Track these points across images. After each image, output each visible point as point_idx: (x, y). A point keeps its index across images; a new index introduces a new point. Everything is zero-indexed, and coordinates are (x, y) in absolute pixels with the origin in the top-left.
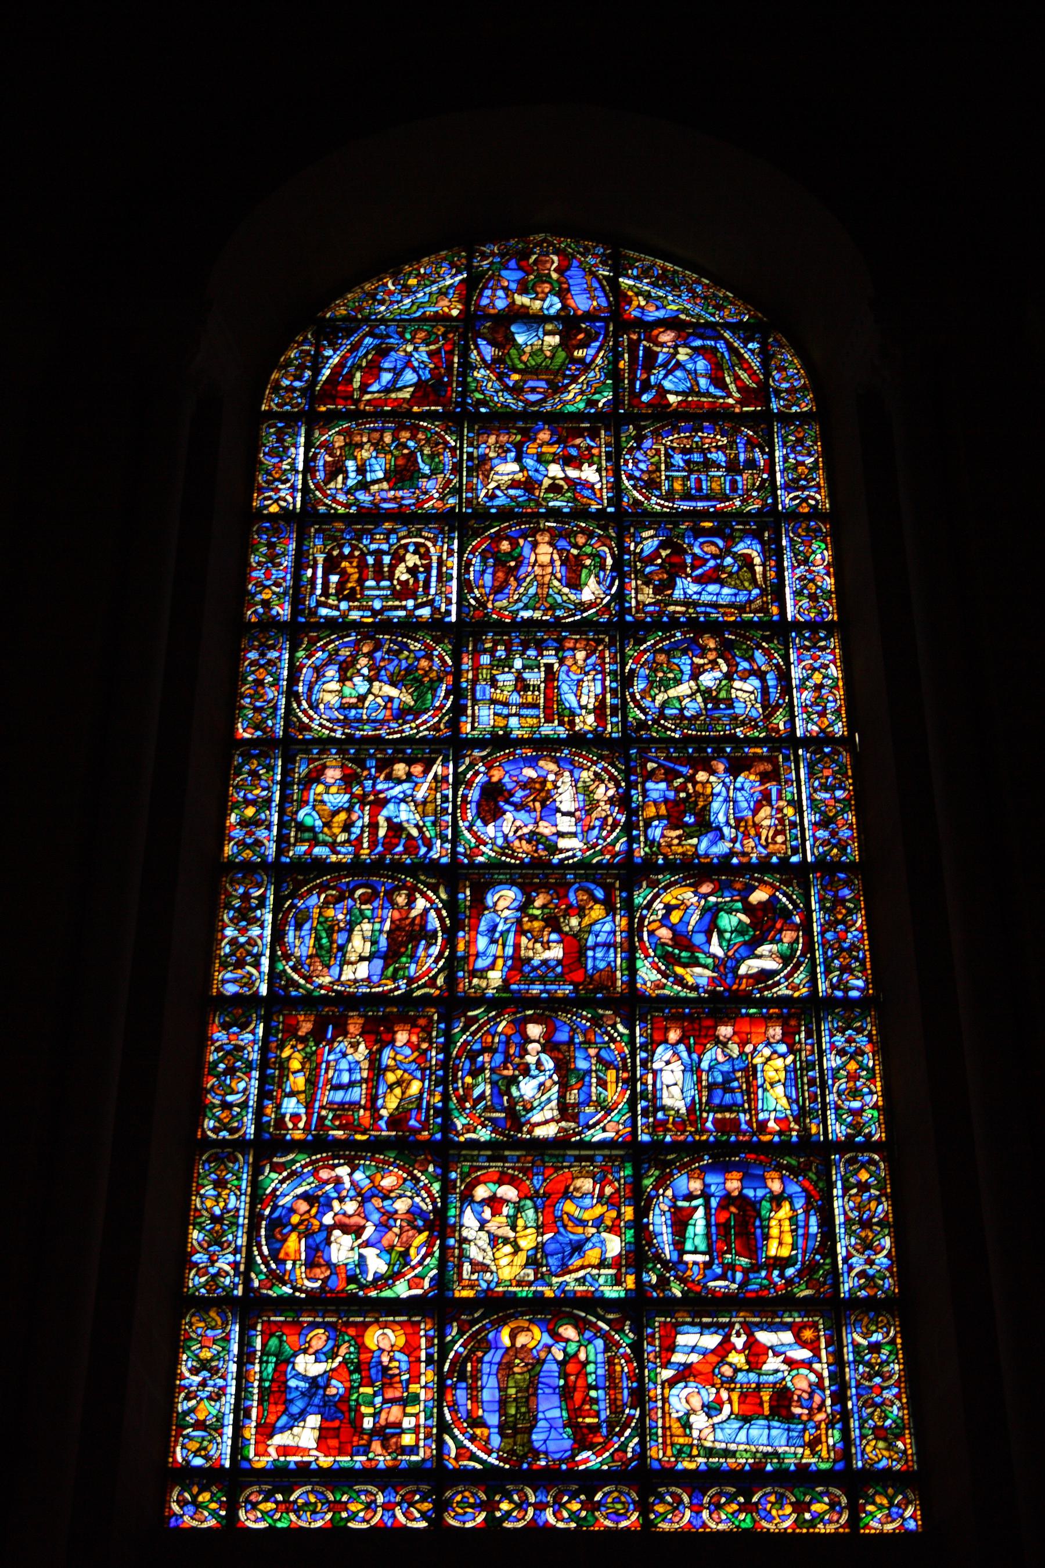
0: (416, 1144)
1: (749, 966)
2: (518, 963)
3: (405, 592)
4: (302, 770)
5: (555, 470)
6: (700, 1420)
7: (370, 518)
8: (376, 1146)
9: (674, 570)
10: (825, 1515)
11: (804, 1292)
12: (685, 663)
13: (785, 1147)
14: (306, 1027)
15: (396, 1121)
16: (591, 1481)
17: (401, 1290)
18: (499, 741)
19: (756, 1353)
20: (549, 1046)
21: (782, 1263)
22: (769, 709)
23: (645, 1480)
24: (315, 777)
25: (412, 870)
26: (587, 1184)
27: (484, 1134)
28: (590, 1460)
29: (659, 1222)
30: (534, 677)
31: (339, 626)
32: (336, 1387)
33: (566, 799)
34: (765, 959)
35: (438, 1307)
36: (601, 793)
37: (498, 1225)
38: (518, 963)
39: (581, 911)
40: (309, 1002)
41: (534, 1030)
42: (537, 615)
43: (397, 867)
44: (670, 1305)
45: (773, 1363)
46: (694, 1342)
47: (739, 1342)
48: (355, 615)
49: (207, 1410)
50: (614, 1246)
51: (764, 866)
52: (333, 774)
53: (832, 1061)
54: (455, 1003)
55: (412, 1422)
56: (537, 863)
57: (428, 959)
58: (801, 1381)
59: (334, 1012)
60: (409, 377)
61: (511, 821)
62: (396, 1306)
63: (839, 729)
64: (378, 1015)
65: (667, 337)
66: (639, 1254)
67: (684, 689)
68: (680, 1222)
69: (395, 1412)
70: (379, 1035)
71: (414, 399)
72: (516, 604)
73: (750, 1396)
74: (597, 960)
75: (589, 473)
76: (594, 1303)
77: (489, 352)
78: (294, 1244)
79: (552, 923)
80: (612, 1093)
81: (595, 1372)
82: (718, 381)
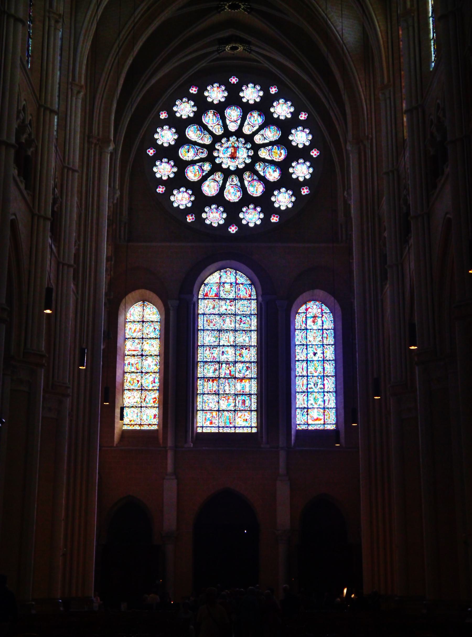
0: (217, 394)
1: (246, 374)
2: (225, 373)
3: (214, 325)
4: (205, 349)
5: (230, 307)
6: (239, 422)
7: (211, 314)
8: (213, 394)
9: (241, 322)
10: (249, 430)
11: (249, 409)
12: (241, 335)
13: (248, 394)
14: (206, 381)
15: (215, 391)
16: (231, 427)
17: (215, 409)
18: (224, 346)
19: (245, 415)
20: (228, 383)
21: (247, 406)
22: (249, 341)
23: (235, 427)
24: (206, 350)
25: (215, 362)
26: (231, 398)
27: (222, 393)
28: (231, 426)
29: (237, 402)
30: (227, 337)
31: (208, 330)
32: (210, 419)
33: (230, 353)
34: (248, 373)
35: (218, 411)
36: (234, 352)
37: (223, 402)
38: (225, 373)
39: (231, 367)
40: (207, 378)
41: (227, 381)
42: (227, 328)
43: (214, 362)
44: (237, 411)
45: (246, 416)
46: (240, 414)
47: (243, 414)
48: (210, 328)
49: (200, 421)
50: (233, 404)
51: (248, 362)
52: (208, 350)
53: (252, 385)
54: (219, 378)
55: (217, 422)
56: (227, 361)
57: (217, 373)
58: (248, 418)
59: (209, 379)
60: (214, 293)
61: (225, 356)
62: (215, 411)
63: (256, 345)
64: (213, 379)
65: (241, 285)
66: (235, 406)
67: (242, 338)
68: (239, 402)
69: (215, 421)
70: (213, 381)
71: (215, 296)
72: (225, 327)
73: (244, 420)
74: (232, 373)
75: (233, 308)
76: (231, 410)
77: (223, 288)
78: (207, 404)
79: (228, 368)
80: (234, 388)
81: (231, 417)
82: (246, 294)
